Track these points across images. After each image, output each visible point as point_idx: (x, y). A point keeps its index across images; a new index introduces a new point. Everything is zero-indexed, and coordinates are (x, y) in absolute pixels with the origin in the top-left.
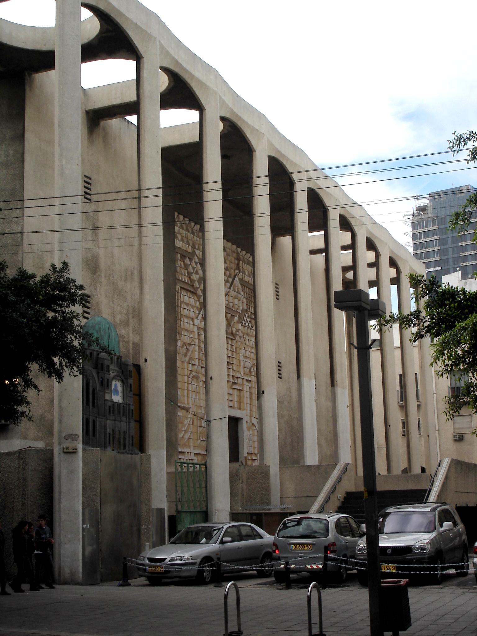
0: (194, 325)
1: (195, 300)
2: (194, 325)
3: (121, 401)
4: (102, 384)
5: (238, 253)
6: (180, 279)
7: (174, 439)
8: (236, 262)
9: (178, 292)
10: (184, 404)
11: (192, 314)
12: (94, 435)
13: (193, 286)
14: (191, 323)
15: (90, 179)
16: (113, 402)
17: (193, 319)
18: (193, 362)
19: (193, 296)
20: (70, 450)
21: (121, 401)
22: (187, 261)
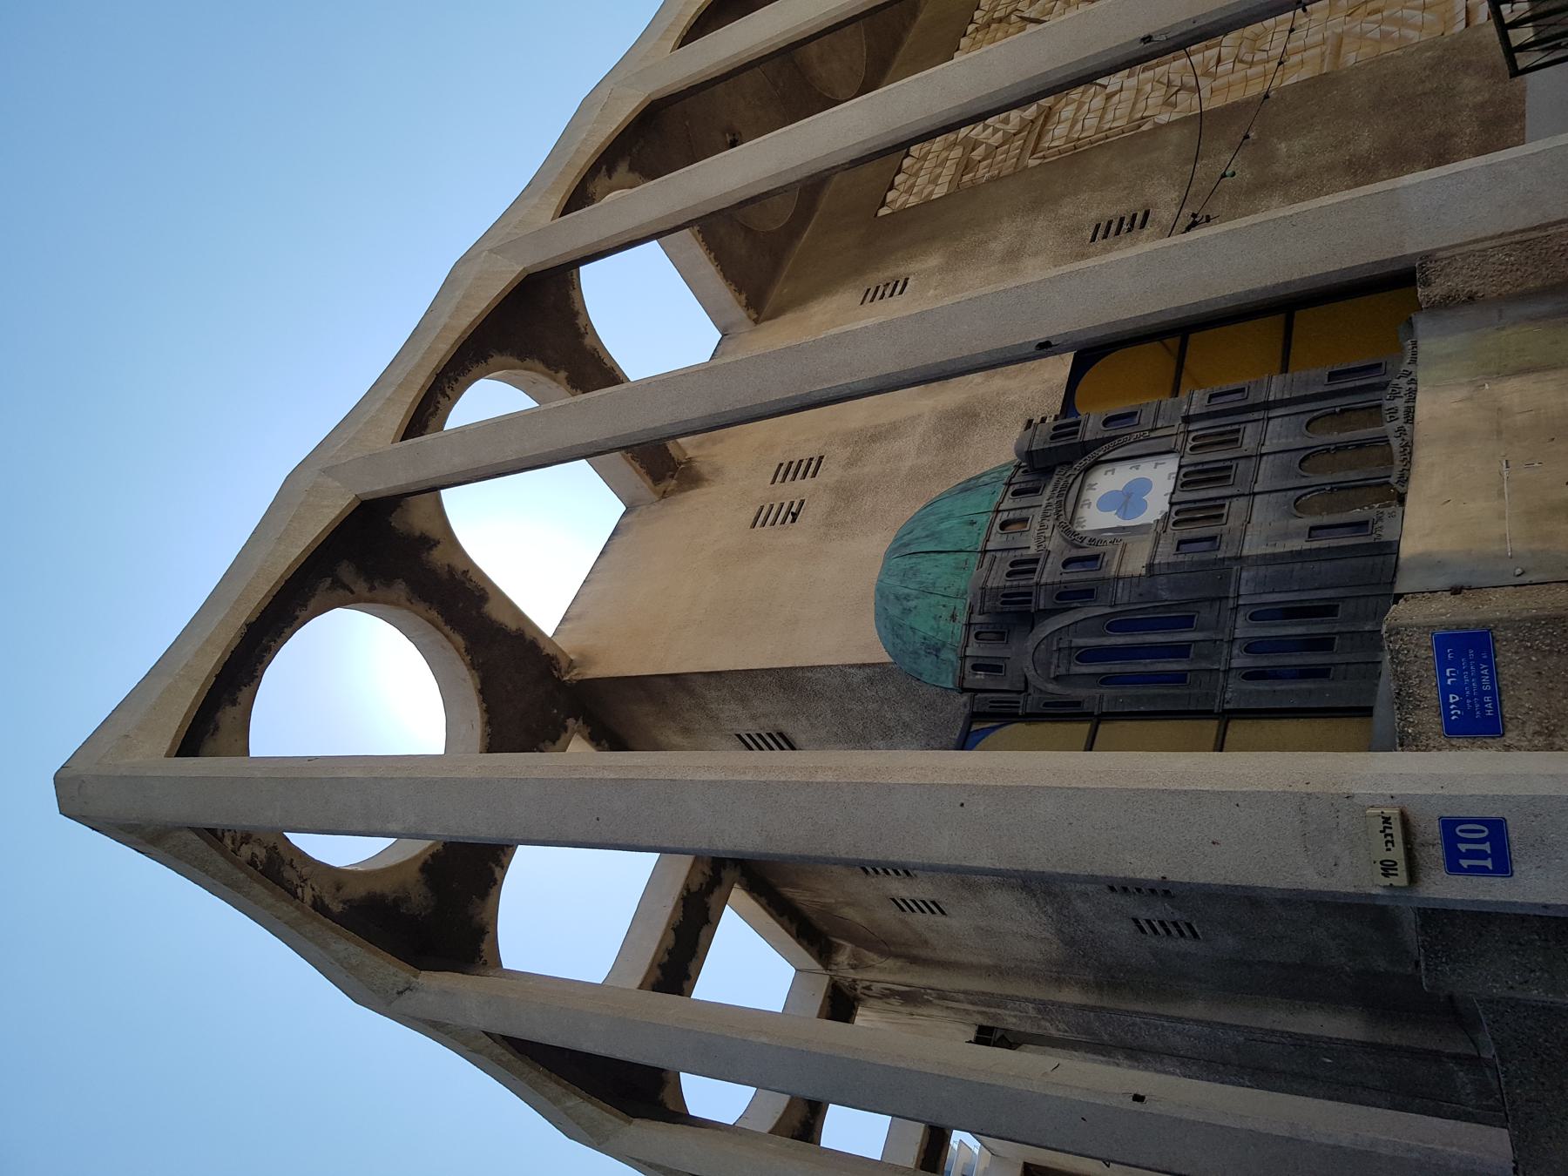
0: (1121, 90)
1: (1067, 105)
2: (1121, 90)
3: (1170, 465)
4: (1086, 594)
5: (977, 30)
6: (1015, 159)
7: (1429, 54)
8: (994, 26)
9: (1044, 157)
10: (1323, 53)
11: (1098, 102)
12: (1325, 610)
13: (1032, 121)
14: (1116, 99)
15: (781, 465)
16: (1167, 516)
17: (1109, 97)
18: (1213, 62)
19: (1055, 114)
20: (1398, 853)
21: (1170, 465)
22: (977, 154)
